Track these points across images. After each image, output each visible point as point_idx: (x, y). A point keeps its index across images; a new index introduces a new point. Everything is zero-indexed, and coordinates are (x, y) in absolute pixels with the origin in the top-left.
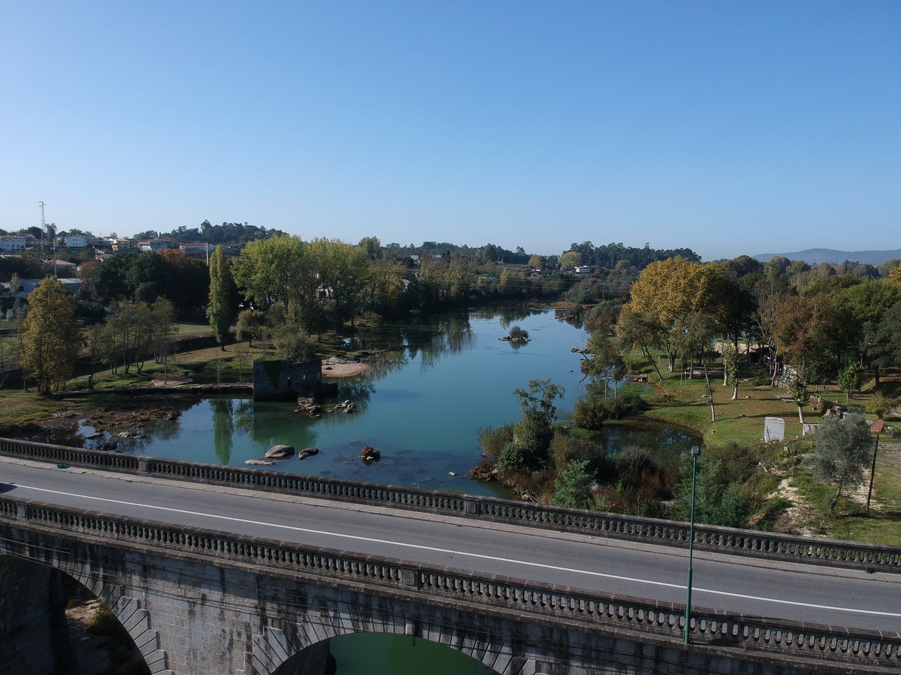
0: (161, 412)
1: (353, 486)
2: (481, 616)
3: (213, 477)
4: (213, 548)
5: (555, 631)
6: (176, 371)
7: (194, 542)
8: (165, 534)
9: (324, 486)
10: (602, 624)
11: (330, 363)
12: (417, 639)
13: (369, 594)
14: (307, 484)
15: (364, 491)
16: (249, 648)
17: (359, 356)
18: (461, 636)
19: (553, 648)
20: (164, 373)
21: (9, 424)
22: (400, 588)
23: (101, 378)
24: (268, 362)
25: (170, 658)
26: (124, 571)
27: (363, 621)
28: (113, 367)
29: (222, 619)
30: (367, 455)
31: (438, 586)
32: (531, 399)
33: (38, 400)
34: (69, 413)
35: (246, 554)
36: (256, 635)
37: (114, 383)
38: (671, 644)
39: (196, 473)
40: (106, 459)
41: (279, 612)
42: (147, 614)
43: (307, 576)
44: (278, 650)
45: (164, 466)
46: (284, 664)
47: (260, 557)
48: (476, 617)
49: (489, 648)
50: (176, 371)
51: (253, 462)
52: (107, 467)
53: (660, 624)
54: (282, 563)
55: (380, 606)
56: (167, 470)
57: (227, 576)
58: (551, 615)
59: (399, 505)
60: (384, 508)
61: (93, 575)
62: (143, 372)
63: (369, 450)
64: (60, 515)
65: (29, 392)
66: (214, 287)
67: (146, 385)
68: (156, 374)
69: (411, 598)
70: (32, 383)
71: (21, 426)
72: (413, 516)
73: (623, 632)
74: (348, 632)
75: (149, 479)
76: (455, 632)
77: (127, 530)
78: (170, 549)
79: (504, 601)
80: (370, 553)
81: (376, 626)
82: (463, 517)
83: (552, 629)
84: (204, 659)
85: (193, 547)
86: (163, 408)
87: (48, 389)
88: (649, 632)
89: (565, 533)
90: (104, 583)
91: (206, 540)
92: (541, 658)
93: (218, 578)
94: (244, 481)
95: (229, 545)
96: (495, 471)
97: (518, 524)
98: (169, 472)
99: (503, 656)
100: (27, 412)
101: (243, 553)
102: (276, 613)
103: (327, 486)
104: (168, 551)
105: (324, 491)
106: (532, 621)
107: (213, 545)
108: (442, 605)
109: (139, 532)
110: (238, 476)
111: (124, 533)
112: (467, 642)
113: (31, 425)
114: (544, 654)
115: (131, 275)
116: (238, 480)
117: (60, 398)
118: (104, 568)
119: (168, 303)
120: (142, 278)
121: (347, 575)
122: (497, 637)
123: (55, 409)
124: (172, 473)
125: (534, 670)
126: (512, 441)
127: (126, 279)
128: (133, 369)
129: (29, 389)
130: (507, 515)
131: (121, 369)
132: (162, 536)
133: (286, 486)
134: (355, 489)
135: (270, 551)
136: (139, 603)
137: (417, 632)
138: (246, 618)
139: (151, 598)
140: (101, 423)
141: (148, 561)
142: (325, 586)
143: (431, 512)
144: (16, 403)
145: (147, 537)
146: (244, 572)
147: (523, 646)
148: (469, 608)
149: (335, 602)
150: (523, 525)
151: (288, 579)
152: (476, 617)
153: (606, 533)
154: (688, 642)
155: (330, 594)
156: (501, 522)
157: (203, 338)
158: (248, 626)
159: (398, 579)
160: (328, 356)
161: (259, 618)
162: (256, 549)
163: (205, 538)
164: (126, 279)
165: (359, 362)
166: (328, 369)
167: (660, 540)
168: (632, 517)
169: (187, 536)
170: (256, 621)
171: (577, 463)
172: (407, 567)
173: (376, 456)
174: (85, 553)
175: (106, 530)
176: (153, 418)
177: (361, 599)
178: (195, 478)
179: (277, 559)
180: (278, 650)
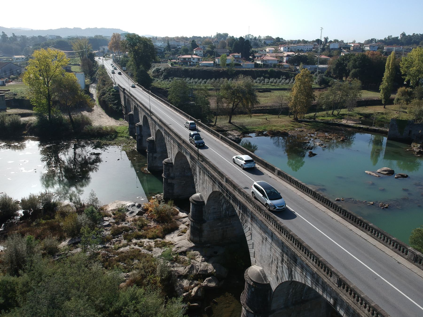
0: (338, 136)
3: (299, 187)
20: (350, 117)
22: (330, 281)
23: (321, 115)
24: (399, 120)
26: (247, 214)
27: (315, 285)
28: (327, 111)
29: (271, 251)
33: (292, 121)
34: (302, 129)
36: (280, 264)
42: (251, 234)
44: (285, 274)
59: (373, 236)
60: (365, 234)
62: (341, 114)
66: (386, 74)
67: (338, 121)
68: (346, 116)
69: (333, 289)
70: (291, 114)
72: (377, 246)
74: (309, 285)
86: (340, 134)
90: (242, 216)
100: (286, 126)
113: (285, 132)
115: (350, 64)
117: (301, 122)
119: (359, 81)
120: (354, 67)
123: (296, 126)
127: (347, 66)
128: (336, 112)
129: (290, 116)
131: (330, 112)
133: (325, 203)
138: (278, 256)
139: (252, 229)
143: (389, 248)
144: (283, 122)
151: (290, 249)
157: (376, 100)
164: (347, 66)
170: (280, 258)
178: (292, 184)
180: (285, 274)
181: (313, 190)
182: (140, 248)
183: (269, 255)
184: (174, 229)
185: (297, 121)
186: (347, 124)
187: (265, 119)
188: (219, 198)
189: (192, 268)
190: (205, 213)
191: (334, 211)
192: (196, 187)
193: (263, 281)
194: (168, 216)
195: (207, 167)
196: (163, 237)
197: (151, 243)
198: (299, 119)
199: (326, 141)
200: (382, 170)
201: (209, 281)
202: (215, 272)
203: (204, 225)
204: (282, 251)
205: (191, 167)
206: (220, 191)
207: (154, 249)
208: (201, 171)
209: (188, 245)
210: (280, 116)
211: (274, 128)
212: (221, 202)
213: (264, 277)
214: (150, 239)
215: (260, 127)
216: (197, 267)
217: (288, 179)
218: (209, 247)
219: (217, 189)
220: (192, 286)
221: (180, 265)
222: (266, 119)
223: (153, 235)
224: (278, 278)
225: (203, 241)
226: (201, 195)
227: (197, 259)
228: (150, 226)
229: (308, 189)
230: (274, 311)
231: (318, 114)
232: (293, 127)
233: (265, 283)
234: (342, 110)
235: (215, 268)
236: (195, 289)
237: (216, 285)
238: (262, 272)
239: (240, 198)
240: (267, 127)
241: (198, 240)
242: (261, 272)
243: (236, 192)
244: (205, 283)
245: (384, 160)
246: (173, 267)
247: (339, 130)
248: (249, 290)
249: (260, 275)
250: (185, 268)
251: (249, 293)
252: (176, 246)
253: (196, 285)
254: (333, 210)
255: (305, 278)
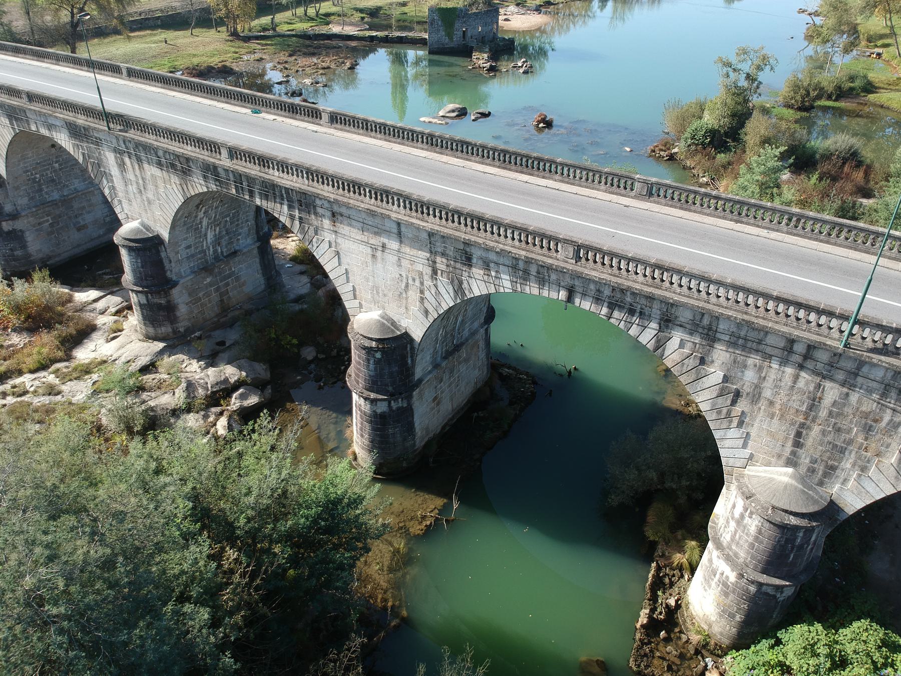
0: (341, 60)
1: (522, 156)
2: (633, 294)
3: (390, 134)
4: (390, 204)
5: (706, 316)
6: (352, 15)
7: (374, 196)
8: (348, 185)
9: (494, 154)
10: (756, 317)
11: (508, 13)
12: (569, 304)
13: (528, 261)
14: (478, 150)
15: (533, 162)
16: (422, 292)
17: (541, 6)
18: (612, 306)
19: (700, 330)
21: (206, 65)
22: (558, 260)
25: (357, 290)
26: (316, 214)
27: (521, 284)
28: (293, 8)
29: (400, 266)
30: (539, 122)
31: (595, 262)
32: (734, 70)
34: (257, 56)
35: (419, 212)
36: (428, 282)
37: (294, 26)
38: (825, 344)
39: (374, 129)
40: (292, 107)
41: (447, 266)
42: (338, 253)
43: (473, 239)
44: (446, 296)
45: (345, 119)
46: (450, 308)
47: (431, 217)
48: (628, 293)
49: (637, 322)
50: (352, 15)
51: (427, 119)
52: (294, 116)
53: (819, 325)
54: (451, 224)
55: (538, 273)
56: (348, 123)
57: (403, 229)
58: (705, 302)
59: (567, 180)
60: (551, 182)
61: (291, 215)
63: (543, 117)
64: (258, 159)
65: (219, 32)
67: (324, 30)
68: (333, 17)
69: (568, 270)
70: (220, 22)
71: (216, 67)
72: (579, 192)
73: (777, 327)
75: (332, 131)
76: (606, 304)
77: (316, 178)
78: (353, 200)
79: (660, 283)
80: (533, 225)
81: (532, 289)
82: (632, 198)
83: (703, 314)
84: (385, 295)
85: (373, 200)
86: (342, 56)
87: (235, 29)
88: (805, 331)
89: (739, 224)
90: (301, 223)
91: (384, 196)
92: (686, 337)
93: (396, 231)
94: (418, 141)
95: (404, 202)
96: (676, 150)
97: (690, 210)
98: (350, 125)
99: (649, 330)
100: (220, 53)
101: (417, 211)
102: (445, 267)
103: (496, 154)
104: (351, 201)
105: (494, 159)
106: (684, 305)
107: (390, 201)
108: (597, 279)
109: (326, 182)
110: (413, 135)
111: (313, 180)
112: (616, 314)
113: (225, 66)
114: (691, 334)
116: (413, 140)
117: (247, 39)
118: (299, 210)
121: (509, 241)
122: (647, 314)
123: (243, 51)
124: (352, 126)
125: (677, 347)
126: (701, 118)
128: (311, 11)
129: (218, 29)
130: (680, 200)
131: (300, 11)
132: (346, 187)
134: (524, 160)
135: (440, 212)
136: (330, 242)
137: (570, 299)
138: (420, 267)
139: (340, 240)
140: (286, 69)
141: (336, 208)
142: (488, 249)
143: (598, 190)
144: (209, 43)
145: (333, 186)
146: (418, 228)
147: (670, 325)
148: (623, 285)
149: (497, 264)
150: (695, 212)
151: (456, 239)
152: (628, 293)
153: (785, 229)
154: (845, 346)
155: (492, 256)
156: (671, 206)
158: (421, 274)
159: (557, 251)
160: (507, 4)
161: (430, 268)
162: (428, 208)
163: (383, 194)
165: (540, 13)
166: (506, 20)
167: (846, 243)
168: (819, 216)
169: (367, 190)
170: (429, 271)
171: (772, 149)
172: (566, 241)
173: (549, 124)
174: (282, 195)
175: (298, 176)
176: (333, 66)
177: (521, 265)
178: (373, 134)
179: (447, 220)
180: (446, 296)
181: (427, 131)
182: (25, 398)
183: (398, 276)
184: (85, 332)
185: (239, 40)
186: (345, 33)
187: (161, 41)
188: (196, 217)
189: (190, 387)
190: (170, 261)
191: (481, 160)
192: (117, 210)
193: (393, 331)
194: (48, 308)
195: (149, 139)
196: (68, 358)
197: (44, 380)
198: (242, 35)
199: (322, 74)
200: (448, 110)
201: (243, 397)
202: (247, 376)
203: (175, 292)
204: (431, 252)
205: (81, 160)
206: (213, 187)
207: (64, 388)
208: (127, 160)
209: (149, 351)
210: (196, 31)
211: (196, 61)
212: (202, 227)
213: (392, 324)
214: (32, 372)
215: (159, 62)
216: (202, 381)
217: (358, 127)
218: (200, 338)
219: (199, 186)
220: (211, 419)
221: (158, 393)
222: (166, 42)
223: (39, 362)
224: (426, 312)
225: (182, 330)
226: (143, 224)
227: (188, 369)
228: (12, 345)
229: (413, 132)
230: (420, 381)
231: (279, 17)
232: (236, 53)
233: (399, 333)
234: (322, 4)
235: (240, 368)
236: (223, 422)
237: (260, 398)
238: (384, 316)
239: (291, 183)
240: (177, 61)
241: (170, 330)
242: (383, 318)
243: (271, 171)
244: (235, 403)
245: (430, 98)
246: (144, 402)
247: (335, 47)
248: (368, 360)
249: (383, 324)
250: (174, 394)
251: (372, 366)
252: (123, 359)
253: (221, 414)
254: (477, 159)
255: (497, 282)
